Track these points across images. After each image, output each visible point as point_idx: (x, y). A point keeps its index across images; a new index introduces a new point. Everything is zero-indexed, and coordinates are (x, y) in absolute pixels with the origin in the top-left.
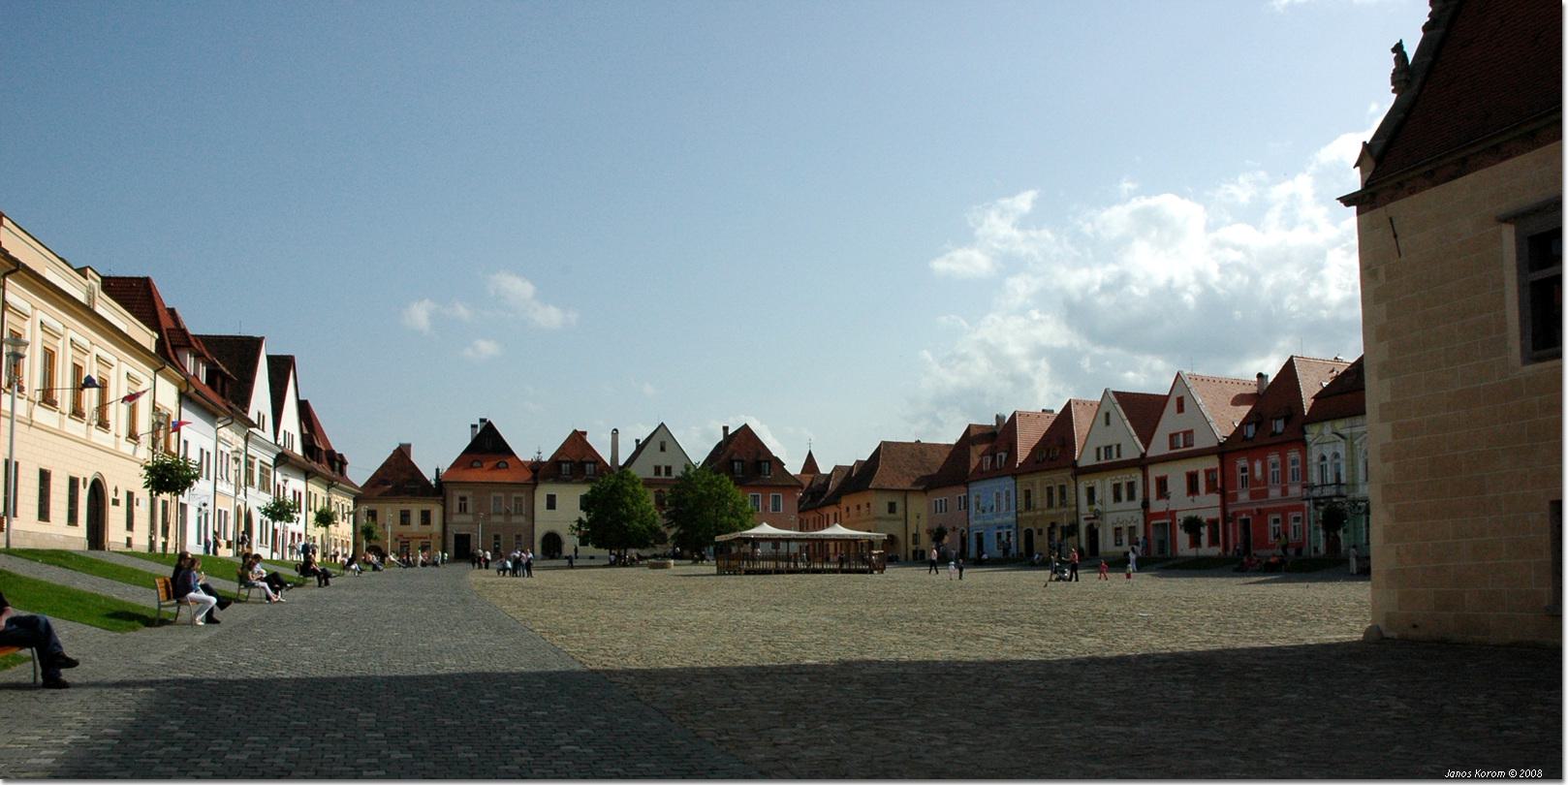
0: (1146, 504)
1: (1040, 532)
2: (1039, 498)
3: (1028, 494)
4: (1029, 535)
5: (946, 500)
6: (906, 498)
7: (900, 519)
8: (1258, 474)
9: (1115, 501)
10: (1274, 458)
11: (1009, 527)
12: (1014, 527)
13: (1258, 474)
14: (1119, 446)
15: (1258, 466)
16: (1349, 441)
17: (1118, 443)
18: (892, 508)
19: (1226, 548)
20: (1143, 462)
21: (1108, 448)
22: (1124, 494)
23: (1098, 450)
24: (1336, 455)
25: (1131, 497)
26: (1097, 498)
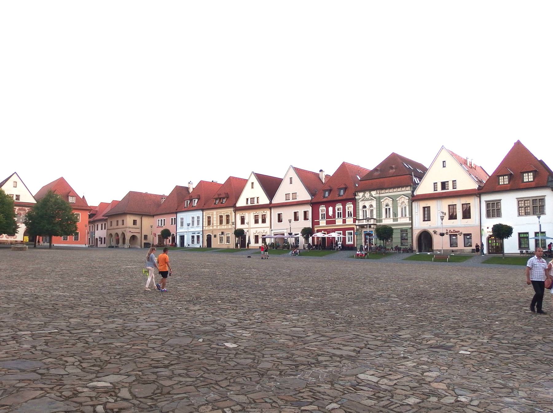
1: (215, 236)
2: (215, 220)
4: (209, 238)
5: (164, 220)
8: (331, 213)
10: (339, 206)
11: (199, 233)
13: (331, 213)
15: (331, 209)
16: (378, 200)
18: (135, 222)
20: (271, 206)
22: (260, 220)
24: (371, 206)
25: (264, 221)
26: (246, 221)
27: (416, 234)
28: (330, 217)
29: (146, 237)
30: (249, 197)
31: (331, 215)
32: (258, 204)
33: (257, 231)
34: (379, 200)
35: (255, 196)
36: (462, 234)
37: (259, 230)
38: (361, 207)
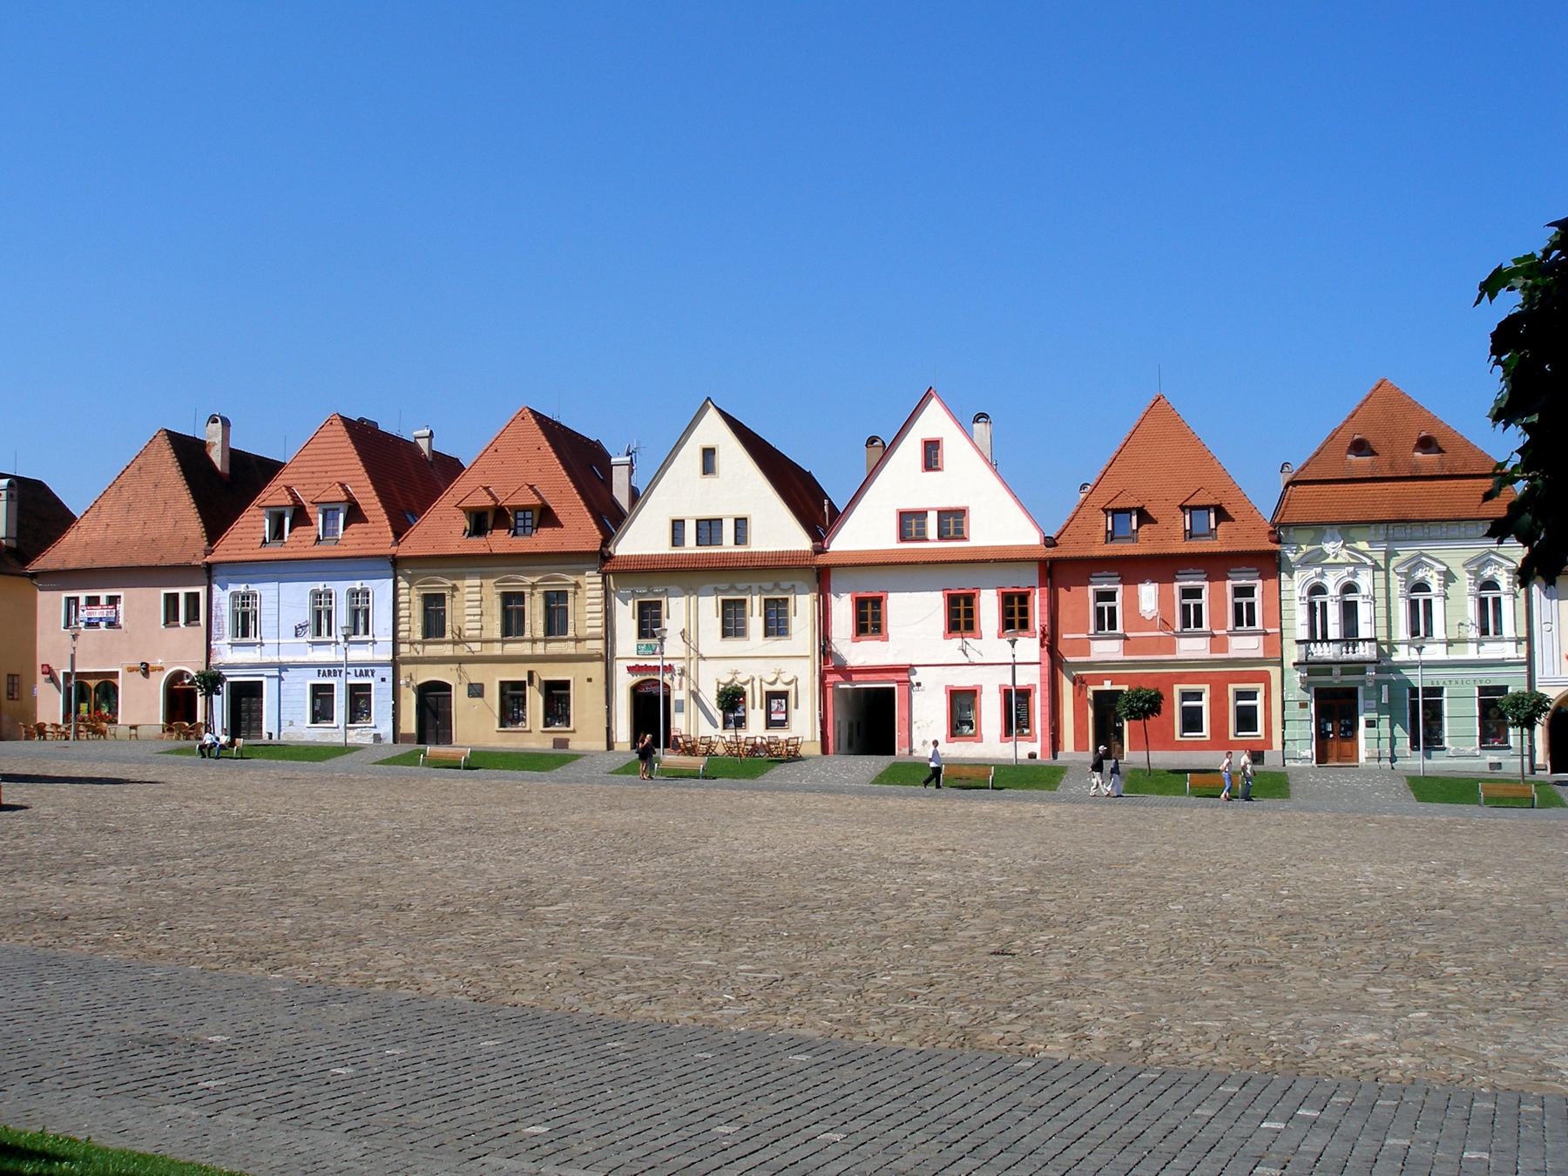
9: (725, 634)
14: (741, 524)
17: (741, 514)
21: (709, 529)
23: (677, 526)
30: (691, 514)
31: (1149, 617)
32: (741, 549)
35: (725, 509)
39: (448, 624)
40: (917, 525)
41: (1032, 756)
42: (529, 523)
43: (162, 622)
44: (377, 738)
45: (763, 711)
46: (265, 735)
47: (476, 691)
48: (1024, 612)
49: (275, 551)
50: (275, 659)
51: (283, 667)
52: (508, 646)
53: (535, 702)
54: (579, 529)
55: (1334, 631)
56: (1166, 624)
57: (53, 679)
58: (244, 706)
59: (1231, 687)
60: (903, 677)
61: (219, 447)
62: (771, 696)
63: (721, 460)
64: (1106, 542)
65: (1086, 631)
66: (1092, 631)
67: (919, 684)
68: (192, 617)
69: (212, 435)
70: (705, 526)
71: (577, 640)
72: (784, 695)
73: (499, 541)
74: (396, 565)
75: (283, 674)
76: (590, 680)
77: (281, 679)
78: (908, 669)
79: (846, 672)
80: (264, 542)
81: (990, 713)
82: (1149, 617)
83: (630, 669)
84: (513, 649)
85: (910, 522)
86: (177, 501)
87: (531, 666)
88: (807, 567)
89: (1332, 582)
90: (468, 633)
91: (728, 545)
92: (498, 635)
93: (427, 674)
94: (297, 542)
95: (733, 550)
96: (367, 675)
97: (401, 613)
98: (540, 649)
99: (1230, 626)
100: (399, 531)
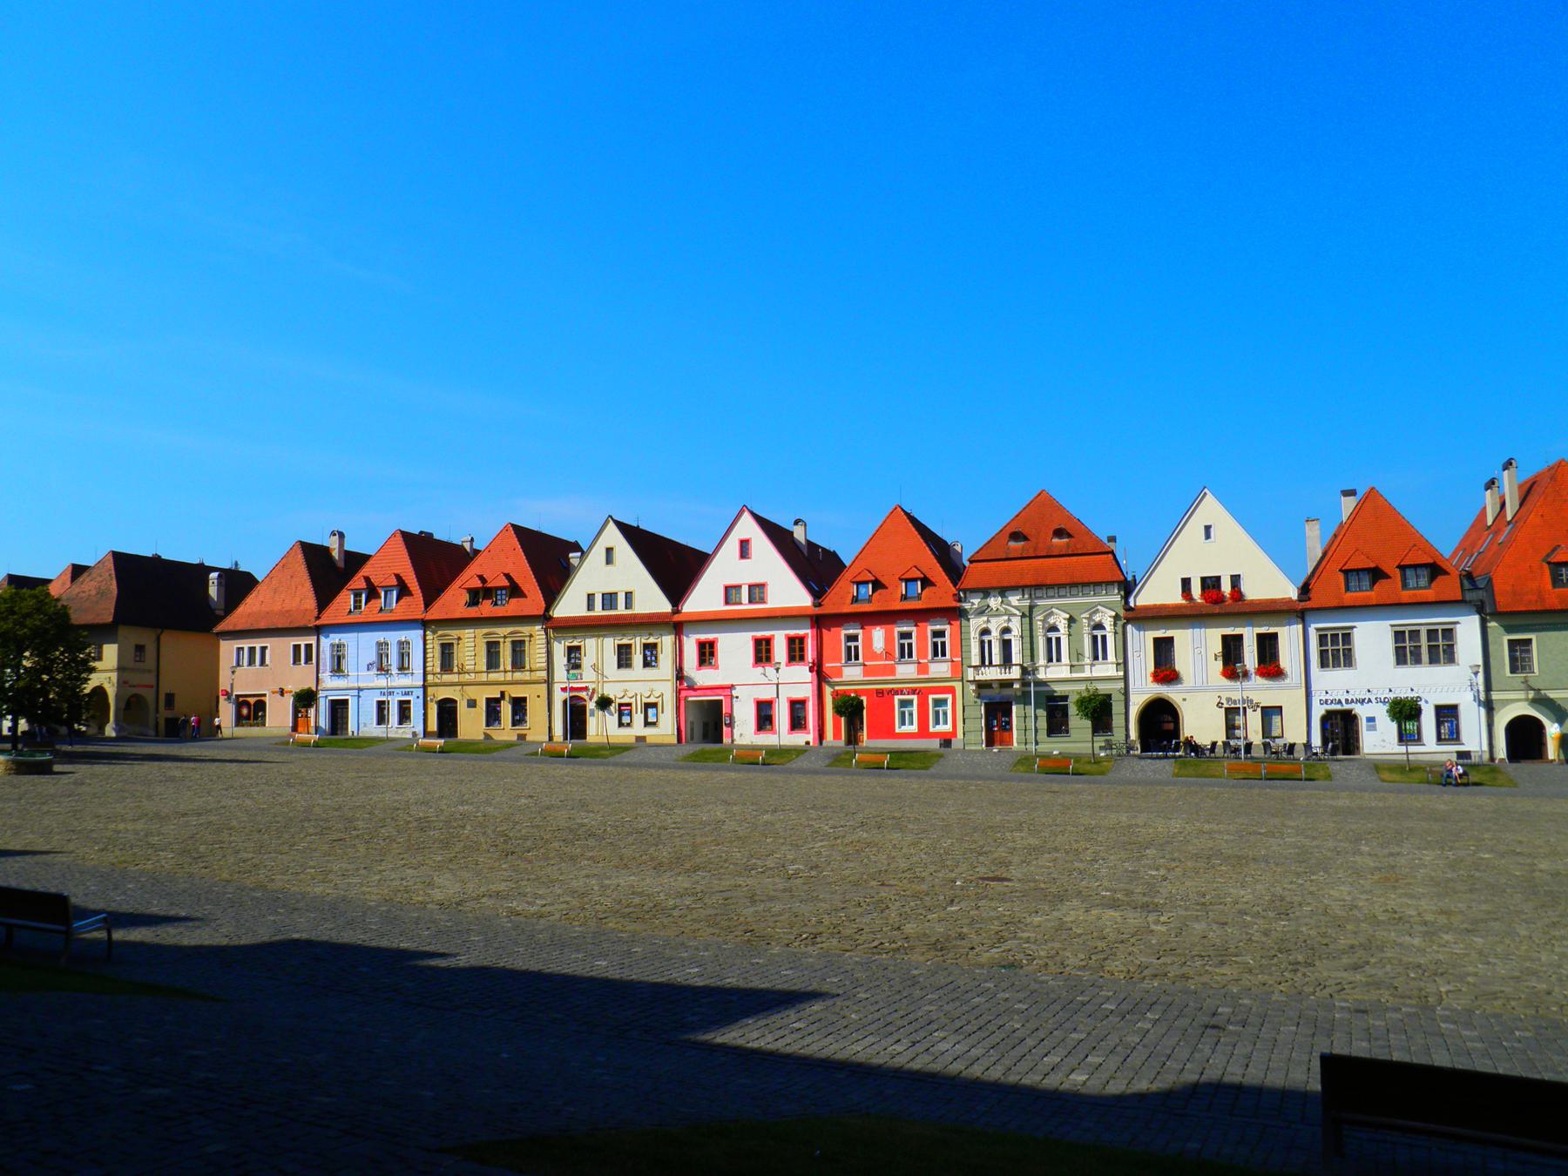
0: (680, 676)
3: (447, 651)
6: (158, 639)
7: (149, 671)
9: (620, 666)
12: (420, 692)
14: (629, 595)
17: (629, 590)
19: (821, 735)
21: (609, 599)
22: (637, 659)
23: (591, 597)
27: (1137, 703)
28: (875, 656)
29: (170, 699)
31: (879, 652)
33: (626, 691)
34: (1028, 615)
36: (1258, 706)
37: (633, 689)
38: (974, 635)
39: (455, 662)
40: (759, 593)
41: (808, 743)
42: (503, 597)
43: (292, 662)
44: (414, 734)
45: (643, 715)
46: (350, 733)
47: (472, 704)
48: (802, 650)
49: (356, 617)
50: (356, 685)
51: (360, 689)
52: (490, 675)
53: (506, 709)
54: (533, 600)
55: (996, 659)
56: (888, 654)
57: (229, 698)
58: (339, 715)
59: (931, 697)
60: (727, 692)
61: (337, 551)
62: (648, 706)
63: (617, 555)
64: (852, 603)
65: (840, 661)
66: (843, 661)
67: (737, 697)
68: (308, 659)
69: (333, 544)
70: (608, 597)
71: (531, 671)
72: (654, 705)
73: (486, 608)
74: (425, 624)
75: (361, 694)
76: (538, 696)
77: (359, 697)
78: (732, 687)
79: (692, 688)
80: (350, 612)
81: (782, 715)
82: (879, 652)
83: (564, 690)
84: (494, 676)
85: (730, 592)
86: (303, 586)
87: (503, 688)
88: (667, 623)
89: (995, 625)
90: (467, 667)
91: (621, 610)
92: (484, 668)
93: (444, 693)
94: (368, 611)
95: (624, 613)
96: (408, 694)
97: (428, 656)
98: (509, 676)
99: (930, 657)
100: (427, 604)
